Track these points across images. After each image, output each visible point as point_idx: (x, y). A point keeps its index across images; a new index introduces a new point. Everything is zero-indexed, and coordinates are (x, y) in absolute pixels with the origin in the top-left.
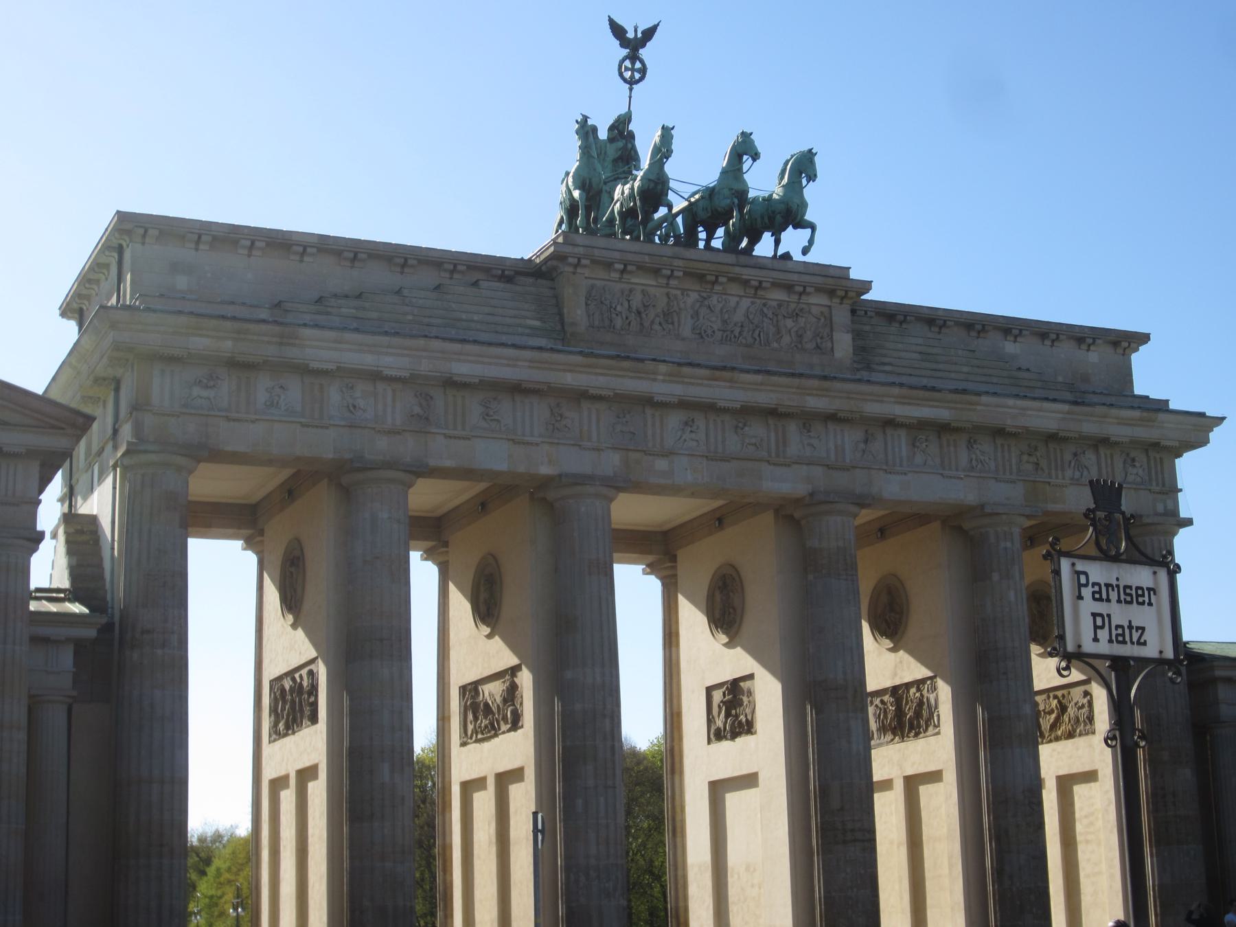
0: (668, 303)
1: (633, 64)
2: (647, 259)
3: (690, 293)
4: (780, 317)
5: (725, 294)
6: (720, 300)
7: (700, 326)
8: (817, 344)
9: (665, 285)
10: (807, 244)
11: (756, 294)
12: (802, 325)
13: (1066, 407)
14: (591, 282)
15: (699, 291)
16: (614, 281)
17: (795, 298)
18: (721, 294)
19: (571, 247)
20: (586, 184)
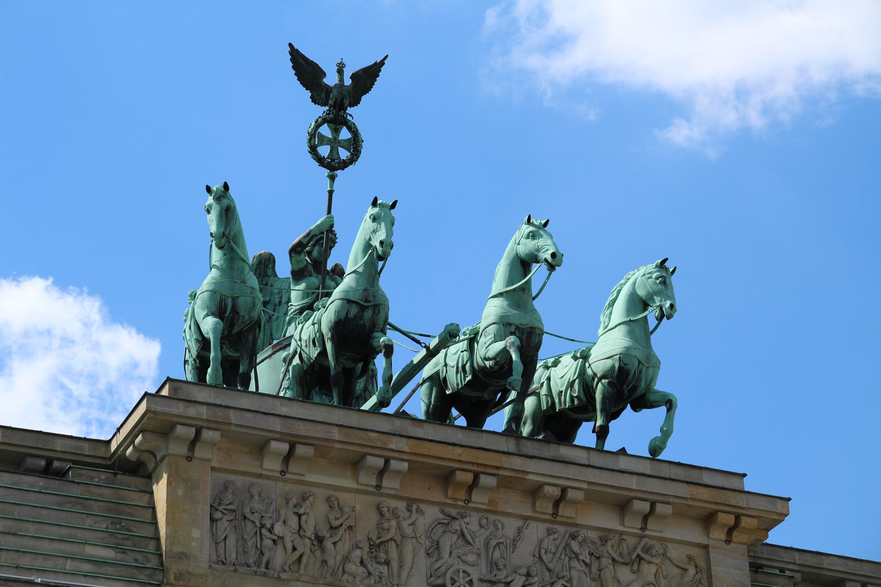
0: (379, 527)
1: (336, 131)
2: (336, 434)
3: (423, 507)
4: (605, 561)
6: (484, 522)
7: (443, 568)
9: (373, 489)
10: (659, 434)
11: (555, 514)
12: (651, 579)
15: (444, 504)
16: (268, 478)
17: (632, 525)
18: (486, 511)
19: (181, 405)
20: (226, 306)
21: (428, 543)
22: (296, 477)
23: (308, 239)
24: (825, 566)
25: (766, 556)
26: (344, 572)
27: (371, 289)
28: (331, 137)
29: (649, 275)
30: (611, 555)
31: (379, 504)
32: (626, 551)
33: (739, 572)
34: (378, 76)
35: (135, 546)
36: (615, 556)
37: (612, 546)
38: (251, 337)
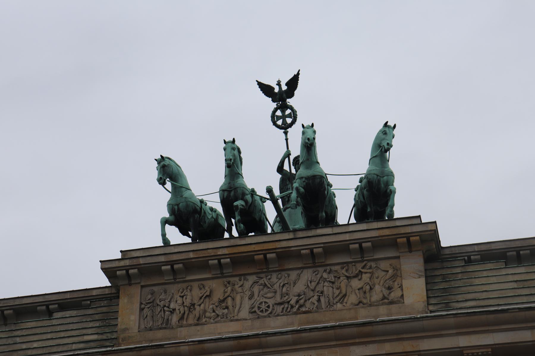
0: (225, 292)
1: (283, 112)
2: (191, 255)
3: (248, 277)
4: (341, 278)
8: (384, 295)
11: (314, 262)
14: (147, 290)
19: (117, 262)
20: (175, 209)
21: (250, 293)
22: (182, 280)
23: (281, 164)
24: (493, 248)
26: (205, 317)
29: (380, 133)
30: (344, 275)
31: (223, 281)
32: (354, 270)
34: (299, 80)
36: (347, 274)
37: (347, 271)
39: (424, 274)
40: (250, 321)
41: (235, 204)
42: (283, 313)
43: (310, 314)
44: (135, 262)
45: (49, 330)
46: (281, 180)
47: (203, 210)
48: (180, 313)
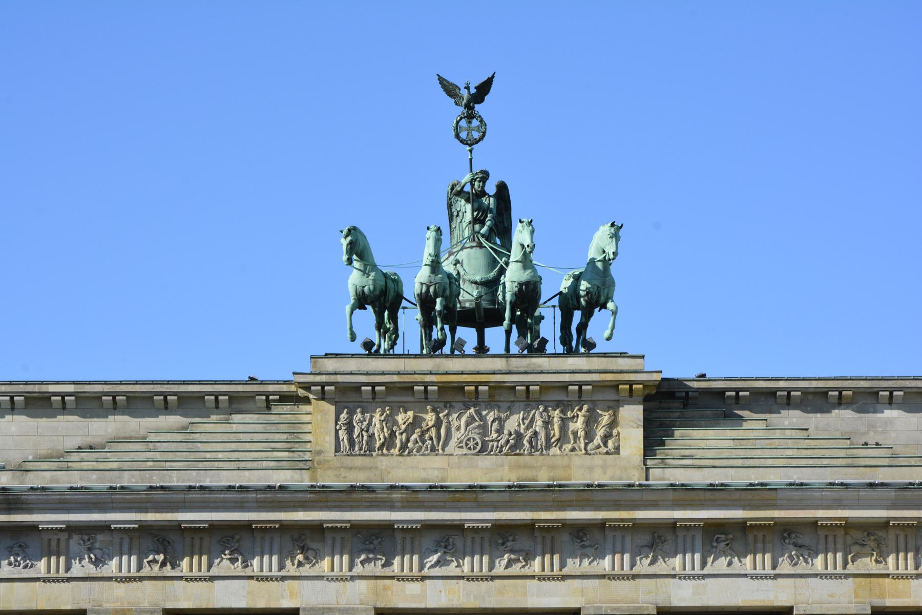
2: (395, 379)
3: (454, 404)
4: (555, 420)
5: (495, 401)
13: (892, 494)
15: (465, 401)
16: (368, 402)
19: (312, 376)
22: (381, 400)
24: (713, 387)
25: (676, 387)
27: (432, 275)
28: (466, 126)
29: (604, 233)
33: (637, 413)
34: (492, 84)
35: (300, 446)
38: (377, 304)
39: (642, 424)
40: (457, 457)
41: (438, 307)
42: (492, 453)
43: (522, 457)
44: (332, 379)
45: (233, 437)
46: (450, 188)
47: (388, 290)
48: (380, 439)
